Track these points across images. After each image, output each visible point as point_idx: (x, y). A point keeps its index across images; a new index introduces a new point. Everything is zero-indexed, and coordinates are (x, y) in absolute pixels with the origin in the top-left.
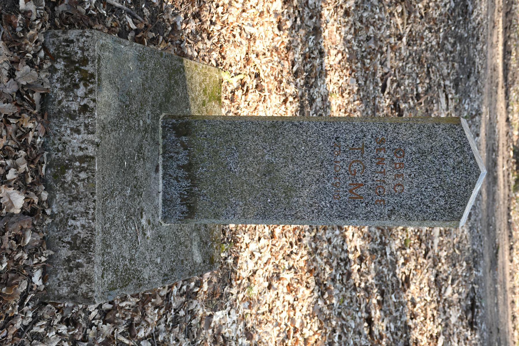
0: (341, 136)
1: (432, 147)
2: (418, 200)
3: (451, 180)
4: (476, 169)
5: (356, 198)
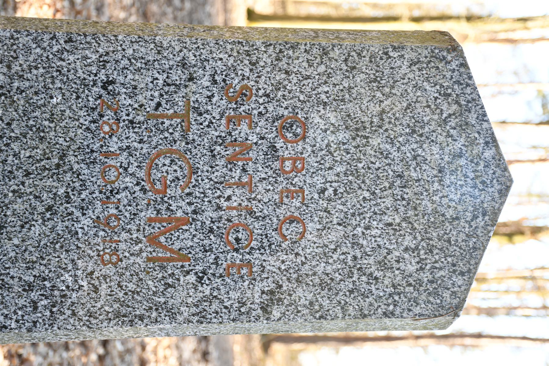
0: (121, 79)
1: (383, 111)
2: (344, 262)
3: (433, 202)
4: (499, 172)
5: (169, 260)
